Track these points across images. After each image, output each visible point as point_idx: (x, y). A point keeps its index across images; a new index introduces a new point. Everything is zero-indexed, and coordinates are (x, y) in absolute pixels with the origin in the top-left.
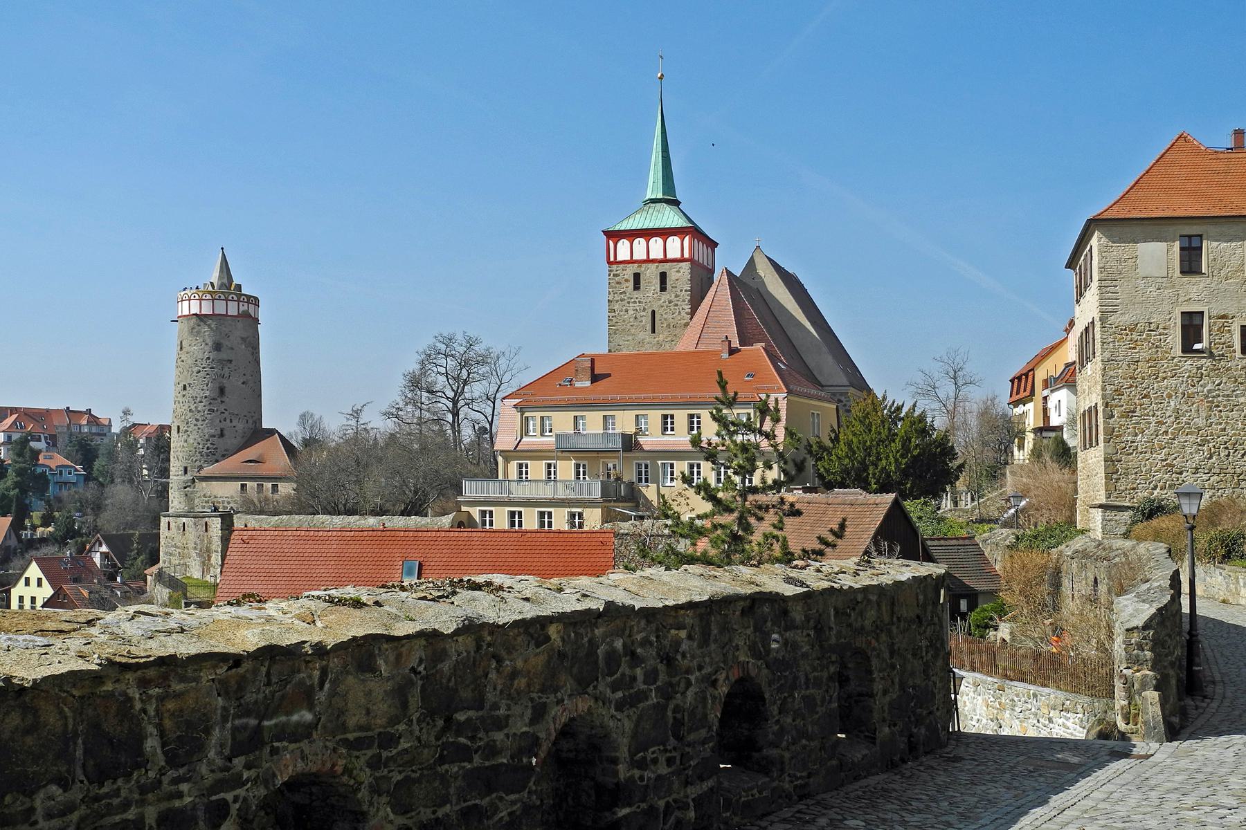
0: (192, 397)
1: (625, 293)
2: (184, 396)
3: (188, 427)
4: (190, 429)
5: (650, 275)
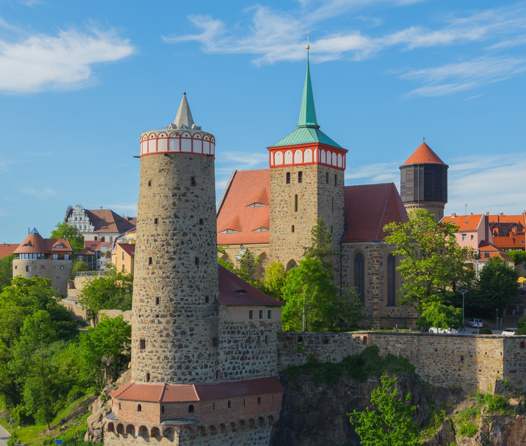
0: (209, 231)
2: (201, 229)
3: (207, 259)
4: (209, 261)
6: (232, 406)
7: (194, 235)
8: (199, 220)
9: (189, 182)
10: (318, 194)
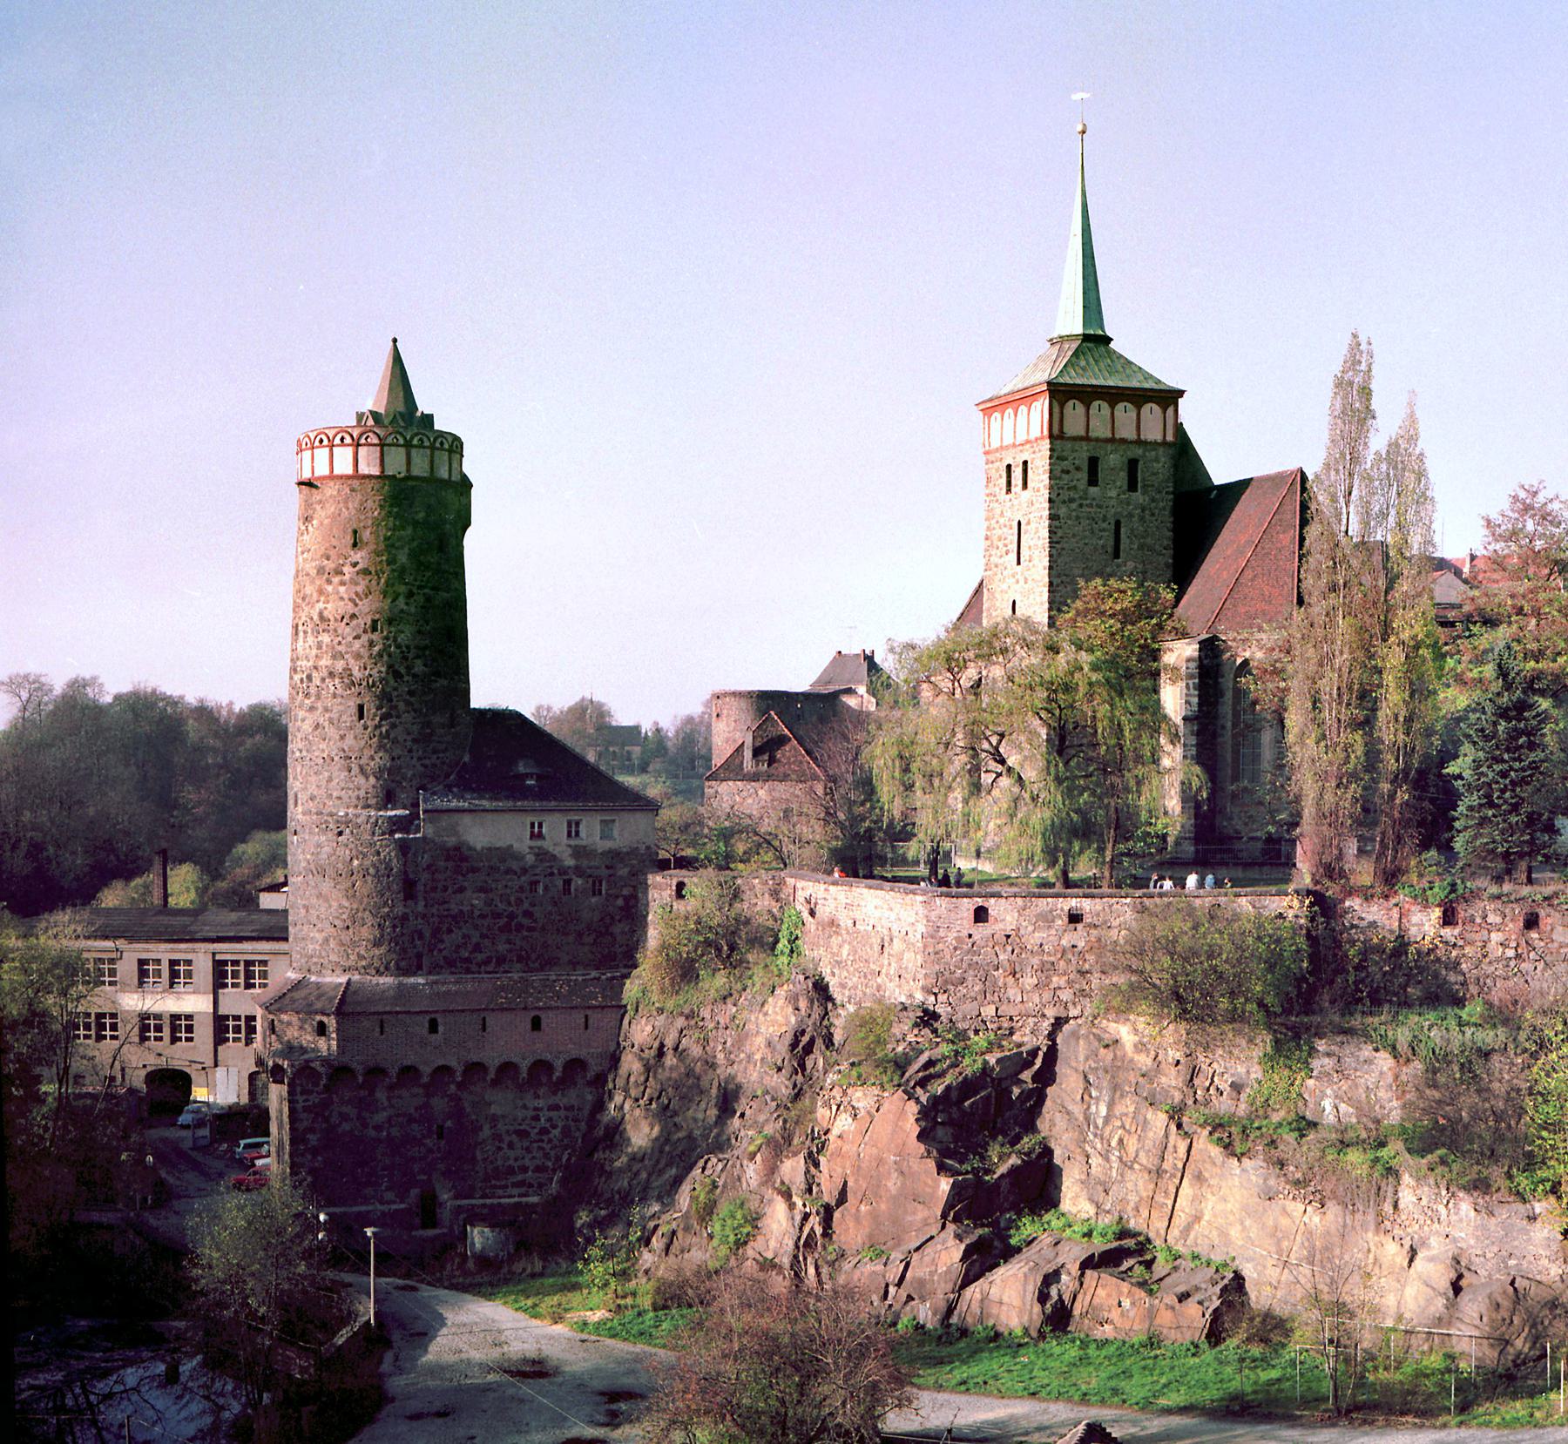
1: (1075, 488)
5: (1113, 460)
6: (441, 1029)
7: (358, 656)
8: (369, 623)
9: (349, 540)
10: (1052, 517)
